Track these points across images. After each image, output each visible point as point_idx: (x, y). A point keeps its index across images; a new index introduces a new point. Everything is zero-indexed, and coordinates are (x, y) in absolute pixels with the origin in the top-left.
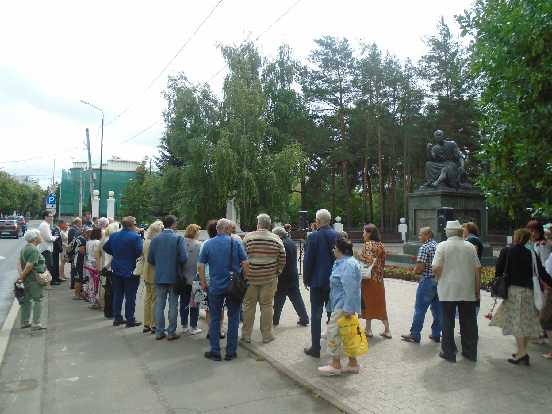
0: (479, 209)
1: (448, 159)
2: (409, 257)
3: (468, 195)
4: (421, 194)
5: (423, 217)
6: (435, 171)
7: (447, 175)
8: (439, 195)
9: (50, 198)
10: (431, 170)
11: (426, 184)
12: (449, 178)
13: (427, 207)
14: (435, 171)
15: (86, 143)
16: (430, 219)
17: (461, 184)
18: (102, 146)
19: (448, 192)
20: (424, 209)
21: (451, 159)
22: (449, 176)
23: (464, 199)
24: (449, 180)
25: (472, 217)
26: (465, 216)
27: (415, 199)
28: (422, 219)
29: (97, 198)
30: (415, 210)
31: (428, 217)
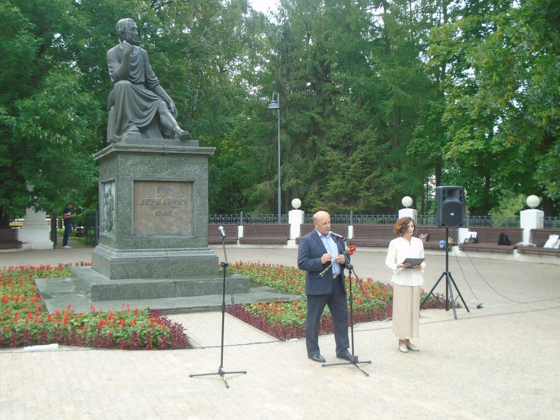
1: (141, 83)
2: (175, 283)
4: (164, 149)
5: (156, 198)
6: (145, 104)
8: (206, 155)
10: (135, 99)
11: (134, 128)
13: (171, 178)
14: (145, 104)
16: (175, 201)
20: (158, 182)
27: (138, 159)
28: (153, 202)
30: (135, 181)
31: (171, 198)
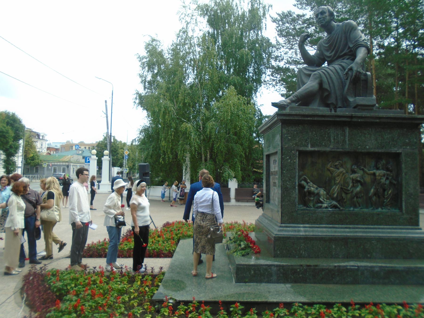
0: (394, 150)
3: (355, 120)
7: (321, 84)
9: (87, 158)
12: (326, 90)
15: (105, 112)
17: (351, 99)
18: (112, 113)
19: (296, 115)
21: (345, 55)
22: (326, 86)
23: (347, 130)
24: (326, 94)
25: (378, 169)
26: (354, 167)
29: (107, 157)
